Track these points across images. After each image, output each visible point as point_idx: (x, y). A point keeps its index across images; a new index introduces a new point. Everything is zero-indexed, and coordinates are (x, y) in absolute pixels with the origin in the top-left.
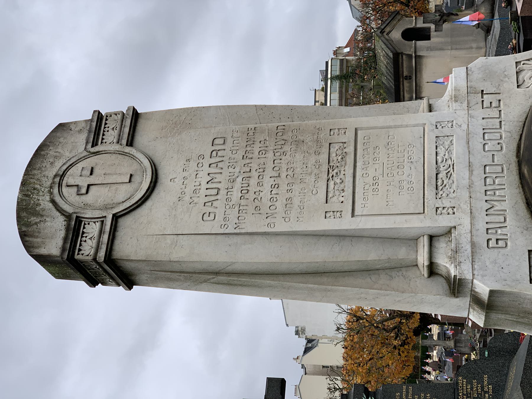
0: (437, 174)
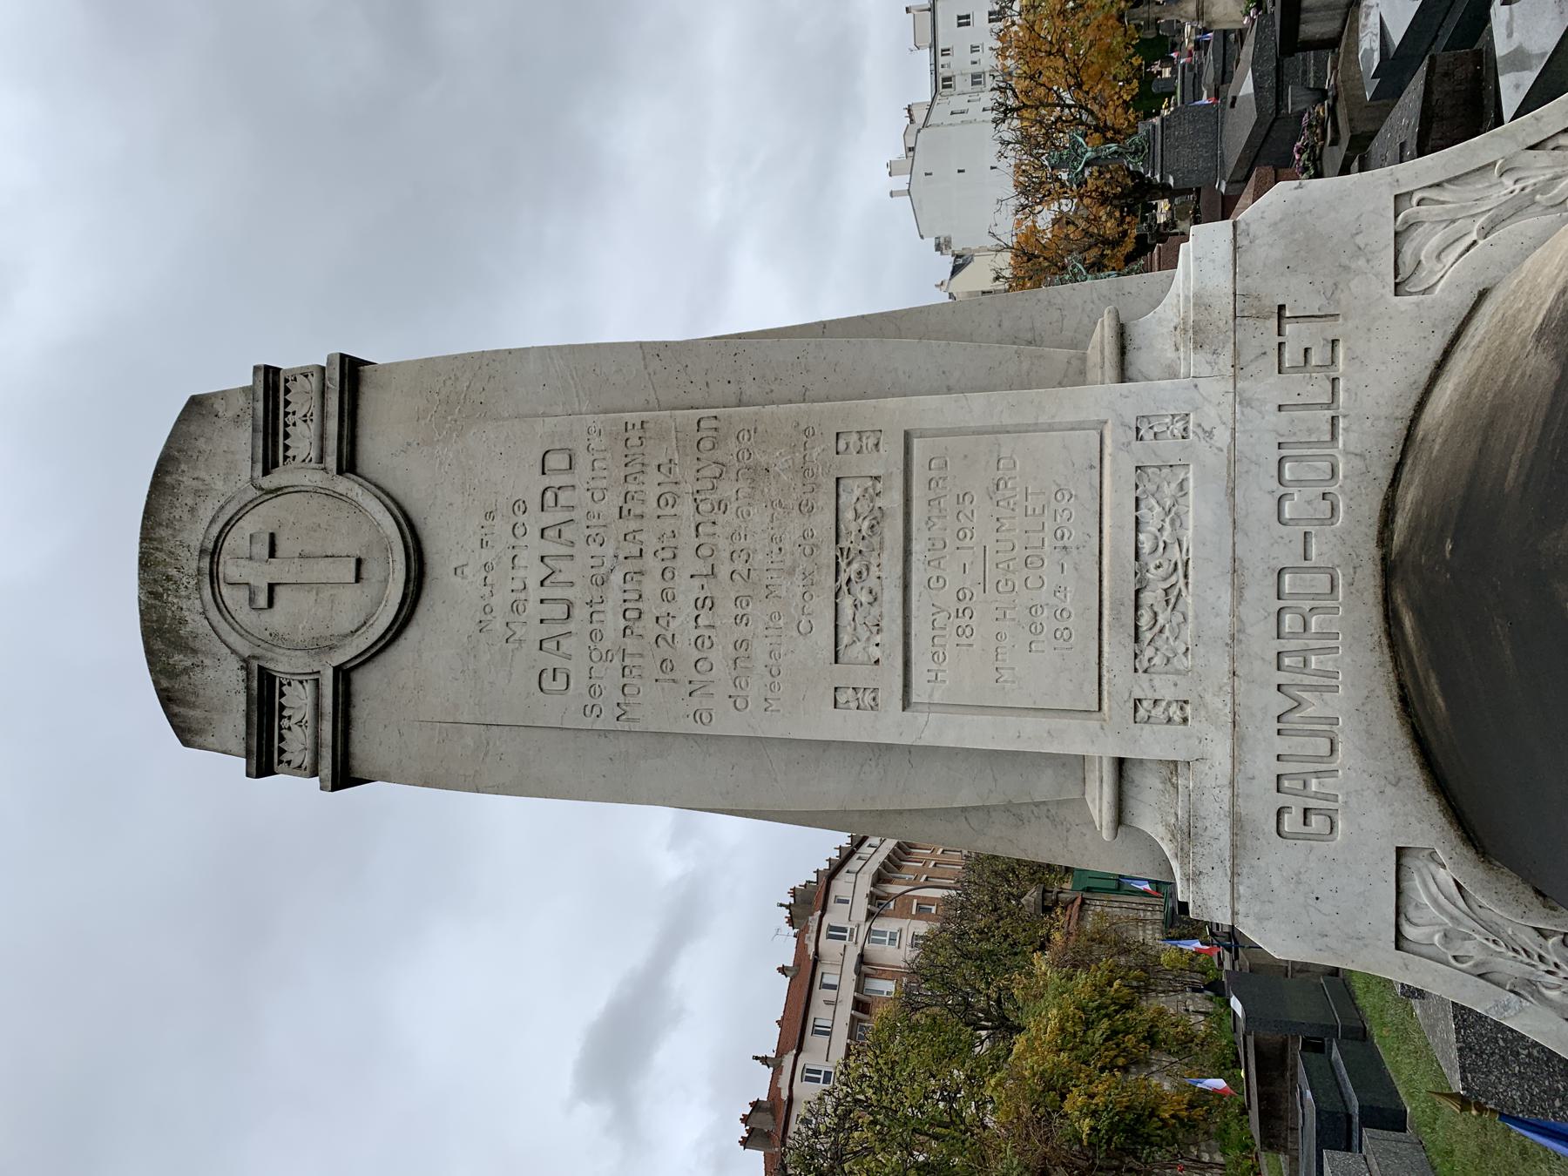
0: (1137, 592)
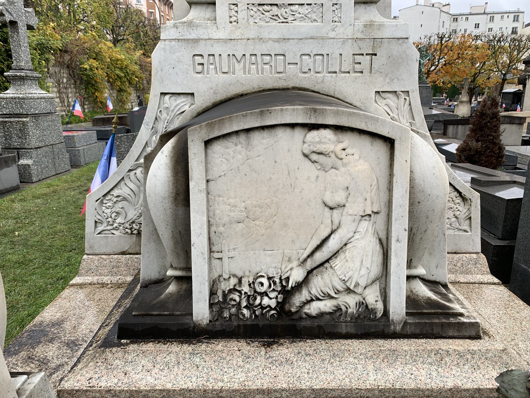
0: (277, 5)
